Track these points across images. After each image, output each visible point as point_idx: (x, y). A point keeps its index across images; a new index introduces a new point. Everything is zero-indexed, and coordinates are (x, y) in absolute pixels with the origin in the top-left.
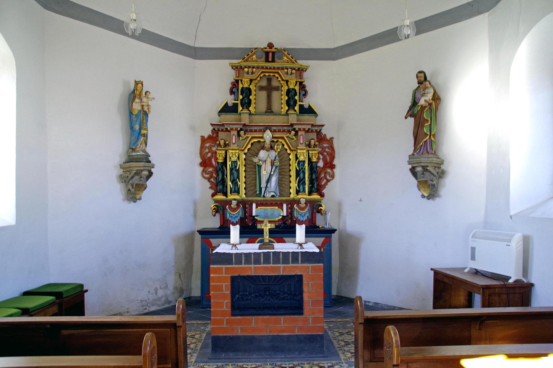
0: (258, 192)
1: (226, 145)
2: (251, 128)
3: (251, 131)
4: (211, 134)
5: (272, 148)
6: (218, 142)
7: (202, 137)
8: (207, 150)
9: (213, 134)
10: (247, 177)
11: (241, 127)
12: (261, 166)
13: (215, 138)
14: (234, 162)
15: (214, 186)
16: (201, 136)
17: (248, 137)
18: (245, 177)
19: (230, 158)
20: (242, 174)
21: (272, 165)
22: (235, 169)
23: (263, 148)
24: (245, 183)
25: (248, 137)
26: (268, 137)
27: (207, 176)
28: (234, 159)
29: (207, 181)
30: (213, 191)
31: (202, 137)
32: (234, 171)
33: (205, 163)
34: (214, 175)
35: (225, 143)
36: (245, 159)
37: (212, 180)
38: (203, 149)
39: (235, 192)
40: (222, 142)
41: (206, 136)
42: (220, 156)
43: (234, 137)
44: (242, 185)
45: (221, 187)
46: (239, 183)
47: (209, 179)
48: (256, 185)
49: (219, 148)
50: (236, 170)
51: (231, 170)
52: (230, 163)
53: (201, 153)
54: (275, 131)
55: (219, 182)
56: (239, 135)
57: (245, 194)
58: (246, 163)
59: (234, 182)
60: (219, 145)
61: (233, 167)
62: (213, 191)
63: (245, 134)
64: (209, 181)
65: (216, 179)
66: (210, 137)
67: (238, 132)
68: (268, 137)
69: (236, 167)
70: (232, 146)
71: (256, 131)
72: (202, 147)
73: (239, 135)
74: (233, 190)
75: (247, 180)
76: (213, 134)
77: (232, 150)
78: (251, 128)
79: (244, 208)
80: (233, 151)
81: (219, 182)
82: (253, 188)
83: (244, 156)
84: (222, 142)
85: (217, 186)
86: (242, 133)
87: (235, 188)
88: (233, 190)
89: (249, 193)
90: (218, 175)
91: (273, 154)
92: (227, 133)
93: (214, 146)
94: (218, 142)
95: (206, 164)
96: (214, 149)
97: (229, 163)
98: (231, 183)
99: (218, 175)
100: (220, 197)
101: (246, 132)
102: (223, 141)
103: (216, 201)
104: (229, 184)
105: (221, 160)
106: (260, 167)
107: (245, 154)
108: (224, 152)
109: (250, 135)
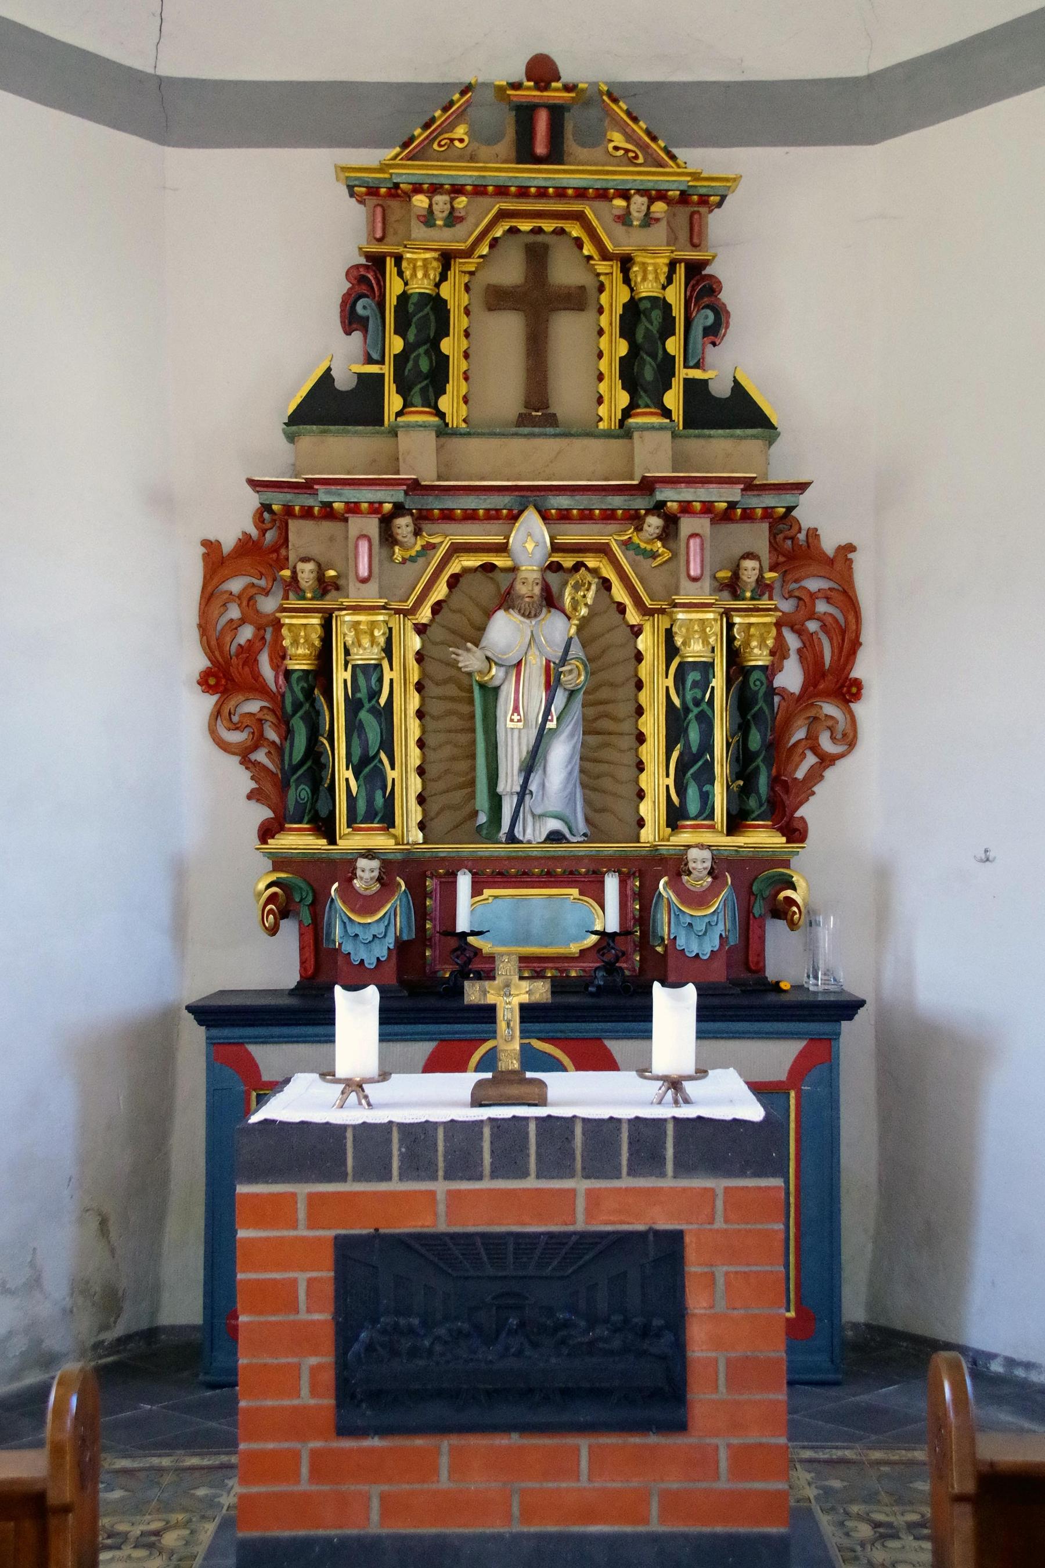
0: (482, 818)
2: (449, 503)
3: (447, 516)
5: (550, 600)
12: (496, 690)
17: (433, 547)
21: (551, 685)
23: (507, 600)
25: (433, 547)
26: (530, 546)
35: (321, 578)
40: (306, 572)
42: (295, 642)
44: (405, 781)
48: (472, 783)
50: (375, 711)
54: (564, 516)
56: (388, 538)
57: (422, 826)
63: (417, 533)
67: (386, 522)
68: (530, 546)
70: (357, 593)
71: (471, 516)
78: (449, 503)
79: (418, 893)
82: (458, 796)
84: (306, 572)
86: (403, 525)
89: (439, 825)
91: (556, 629)
100: (299, 841)
101: (422, 518)
103: (280, 862)
106: (491, 693)
108: (315, 621)
109: (443, 537)
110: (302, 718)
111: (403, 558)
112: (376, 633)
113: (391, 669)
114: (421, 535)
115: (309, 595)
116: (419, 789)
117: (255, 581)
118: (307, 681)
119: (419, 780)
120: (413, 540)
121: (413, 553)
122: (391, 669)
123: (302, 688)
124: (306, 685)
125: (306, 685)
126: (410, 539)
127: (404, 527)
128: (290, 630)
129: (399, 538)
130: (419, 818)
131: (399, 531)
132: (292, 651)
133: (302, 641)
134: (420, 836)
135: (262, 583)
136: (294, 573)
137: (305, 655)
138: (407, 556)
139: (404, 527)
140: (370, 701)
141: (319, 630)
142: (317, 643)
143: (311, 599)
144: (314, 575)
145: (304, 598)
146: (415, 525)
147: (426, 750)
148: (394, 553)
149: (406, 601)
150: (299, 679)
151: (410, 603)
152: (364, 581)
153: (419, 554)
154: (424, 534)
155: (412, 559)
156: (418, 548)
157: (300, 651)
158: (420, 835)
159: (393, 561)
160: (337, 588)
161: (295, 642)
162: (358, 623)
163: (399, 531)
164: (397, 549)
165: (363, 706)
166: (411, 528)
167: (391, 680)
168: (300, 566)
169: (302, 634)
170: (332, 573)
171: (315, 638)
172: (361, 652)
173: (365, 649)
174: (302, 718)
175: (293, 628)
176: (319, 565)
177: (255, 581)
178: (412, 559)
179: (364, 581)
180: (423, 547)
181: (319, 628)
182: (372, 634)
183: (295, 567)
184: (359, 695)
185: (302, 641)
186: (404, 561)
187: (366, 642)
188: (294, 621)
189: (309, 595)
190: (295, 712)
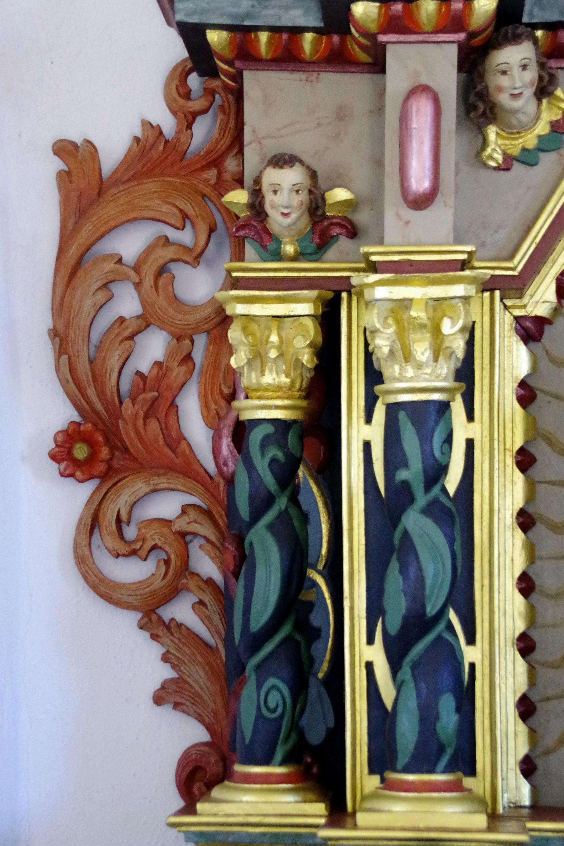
1: (325, 227)
4: (167, 123)
6: (238, 197)
7: (74, 156)
8: (127, 303)
9: (188, 120)
10: (546, 580)
13: (214, 160)
14: (417, 410)
15: (198, 676)
16: (63, 149)
18: (526, 585)
19: (374, 376)
20: (502, 552)
22: (423, 501)
24: (526, 645)
27: (132, 572)
28: (419, 377)
29: (129, 620)
30: (197, 734)
31: (74, 156)
32: (415, 522)
33: (103, 444)
34: (207, 566)
35: (316, 207)
36: (527, 394)
37: (182, 611)
38: (86, 296)
39: (424, 761)
40: (284, 191)
41: (113, 147)
42: (258, 358)
43: (422, 115)
45: (276, 693)
46: (471, 654)
47: (150, 611)
49: (254, 265)
51: (386, 507)
52: (375, 432)
53: (61, 338)
55: (256, 641)
56: (478, 105)
57: (528, 768)
58: (533, 430)
59: (425, 640)
60: (255, 225)
61: (413, 473)
62: (197, 734)
63: (544, 90)
64: (152, 622)
65: (225, 599)
66: (153, 155)
67: (473, 60)
69: (436, 472)
70: (401, 234)
72: (74, 266)
73: (478, 105)
74: (407, 731)
75: (550, 611)
76: (188, 120)
77: (403, 269)
80: (417, 291)
81: (256, 641)
83: (517, 360)
84: (284, 191)
85: (231, 675)
87: (428, 718)
88: (407, 731)
90: (240, 562)
92: (348, 87)
93: (196, 257)
94: (238, 197)
95: (113, 438)
96: (197, 286)
97: (360, 433)
98: (376, 654)
99: (240, 562)
102: (291, 177)
104: (364, 652)
105: (270, 395)
107: (531, 331)
108: (304, 307)
110: (270, 527)
112: (447, 327)
113: (470, 417)
115: (289, 249)
116: (522, 688)
117: (172, 234)
118: (283, 445)
119: (521, 665)
122: (470, 417)
123: (273, 461)
124: (280, 455)
125: (280, 455)
126: (526, 103)
127: (516, 71)
128: (244, 329)
129: (504, 99)
130: (523, 750)
131: (504, 81)
132: (249, 379)
133: (273, 354)
134: (523, 792)
135: (185, 237)
136: (257, 193)
137: (279, 388)
138: (515, 151)
139: (516, 71)
140: (428, 487)
141: (311, 326)
142: (307, 358)
143: (294, 259)
144: (304, 196)
145: (278, 256)
146: (542, 66)
147: (534, 597)
148: (485, 143)
149: (511, 257)
150: (265, 442)
151: (519, 262)
152: (421, 202)
155: (528, 158)
156: (542, 128)
157: (269, 379)
158: (525, 788)
159: (485, 165)
160: (353, 232)
161: (258, 358)
162: (405, 304)
163: (504, 81)
164: (492, 132)
165: (412, 500)
167: (470, 443)
168: (272, 176)
169: (274, 338)
170: (340, 194)
171: (303, 344)
172: (410, 372)
173: (419, 366)
174: (270, 527)
175: (254, 327)
176: (313, 175)
177: (172, 234)
179: (421, 202)
181: (310, 324)
182: (436, 332)
183: (258, 181)
184: (402, 475)
185: (273, 354)
186: (509, 162)
187: (422, 350)
188: (256, 309)
189: (289, 249)
190: (256, 517)
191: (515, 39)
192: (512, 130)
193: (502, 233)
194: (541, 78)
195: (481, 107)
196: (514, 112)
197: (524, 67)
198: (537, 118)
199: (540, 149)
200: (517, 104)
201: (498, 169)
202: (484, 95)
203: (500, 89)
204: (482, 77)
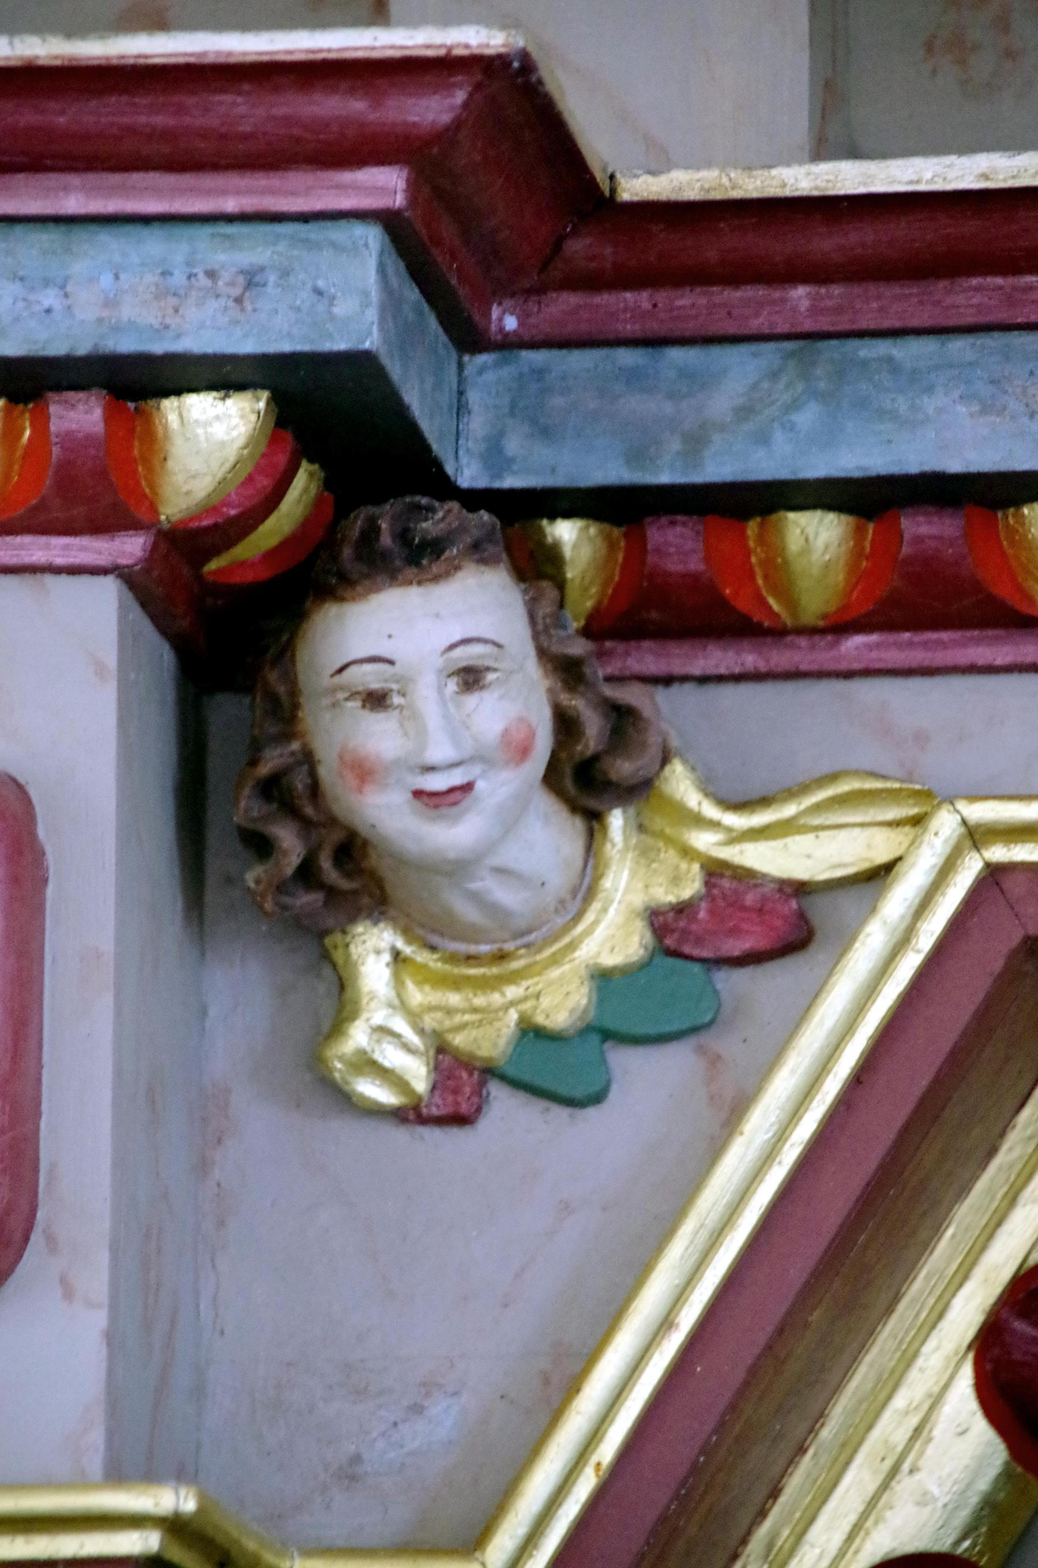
11: (332, 287)
17: (791, 926)
25: (791, 926)
63: (592, 775)
111: (450, 1064)
114: (639, 791)
120: (547, 837)
121: (560, 998)
126: (507, 833)
127: (429, 694)
129: (385, 813)
131: (379, 737)
138: (491, 1040)
139: (429, 694)
146: (567, 671)
148: (341, 1001)
153: (626, 1016)
154: (681, 784)
155: (557, 1070)
156: (612, 935)
163: (379, 737)
164: (373, 953)
166: (519, 703)
178: (557, 1070)
180: (668, 926)
186: (458, 1094)
191: (420, 559)
192: (466, 944)
193: (443, 1421)
194: (565, 725)
195: (290, 844)
196: (457, 869)
197: (471, 678)
198: (585, 890)
199: (603, 1033)
200: (454, 835)
201: (411, 1115)
202: (295, 792)
203: (364, 772)
204: (284, 714)
